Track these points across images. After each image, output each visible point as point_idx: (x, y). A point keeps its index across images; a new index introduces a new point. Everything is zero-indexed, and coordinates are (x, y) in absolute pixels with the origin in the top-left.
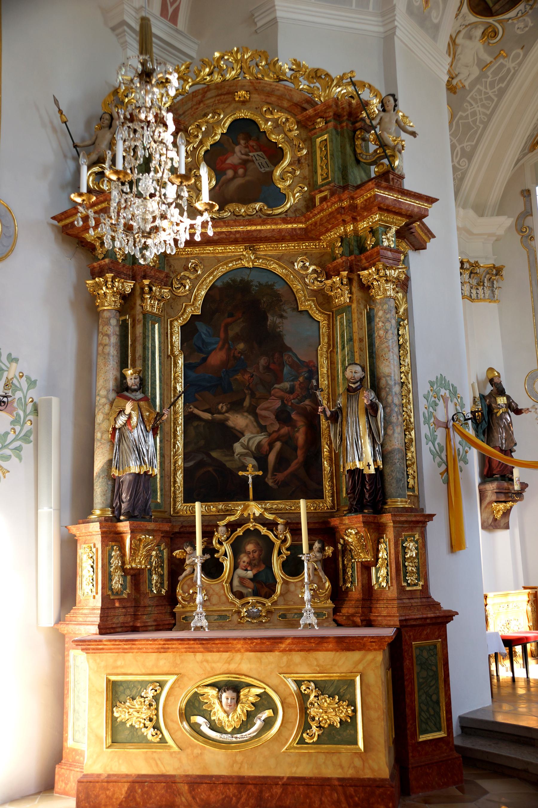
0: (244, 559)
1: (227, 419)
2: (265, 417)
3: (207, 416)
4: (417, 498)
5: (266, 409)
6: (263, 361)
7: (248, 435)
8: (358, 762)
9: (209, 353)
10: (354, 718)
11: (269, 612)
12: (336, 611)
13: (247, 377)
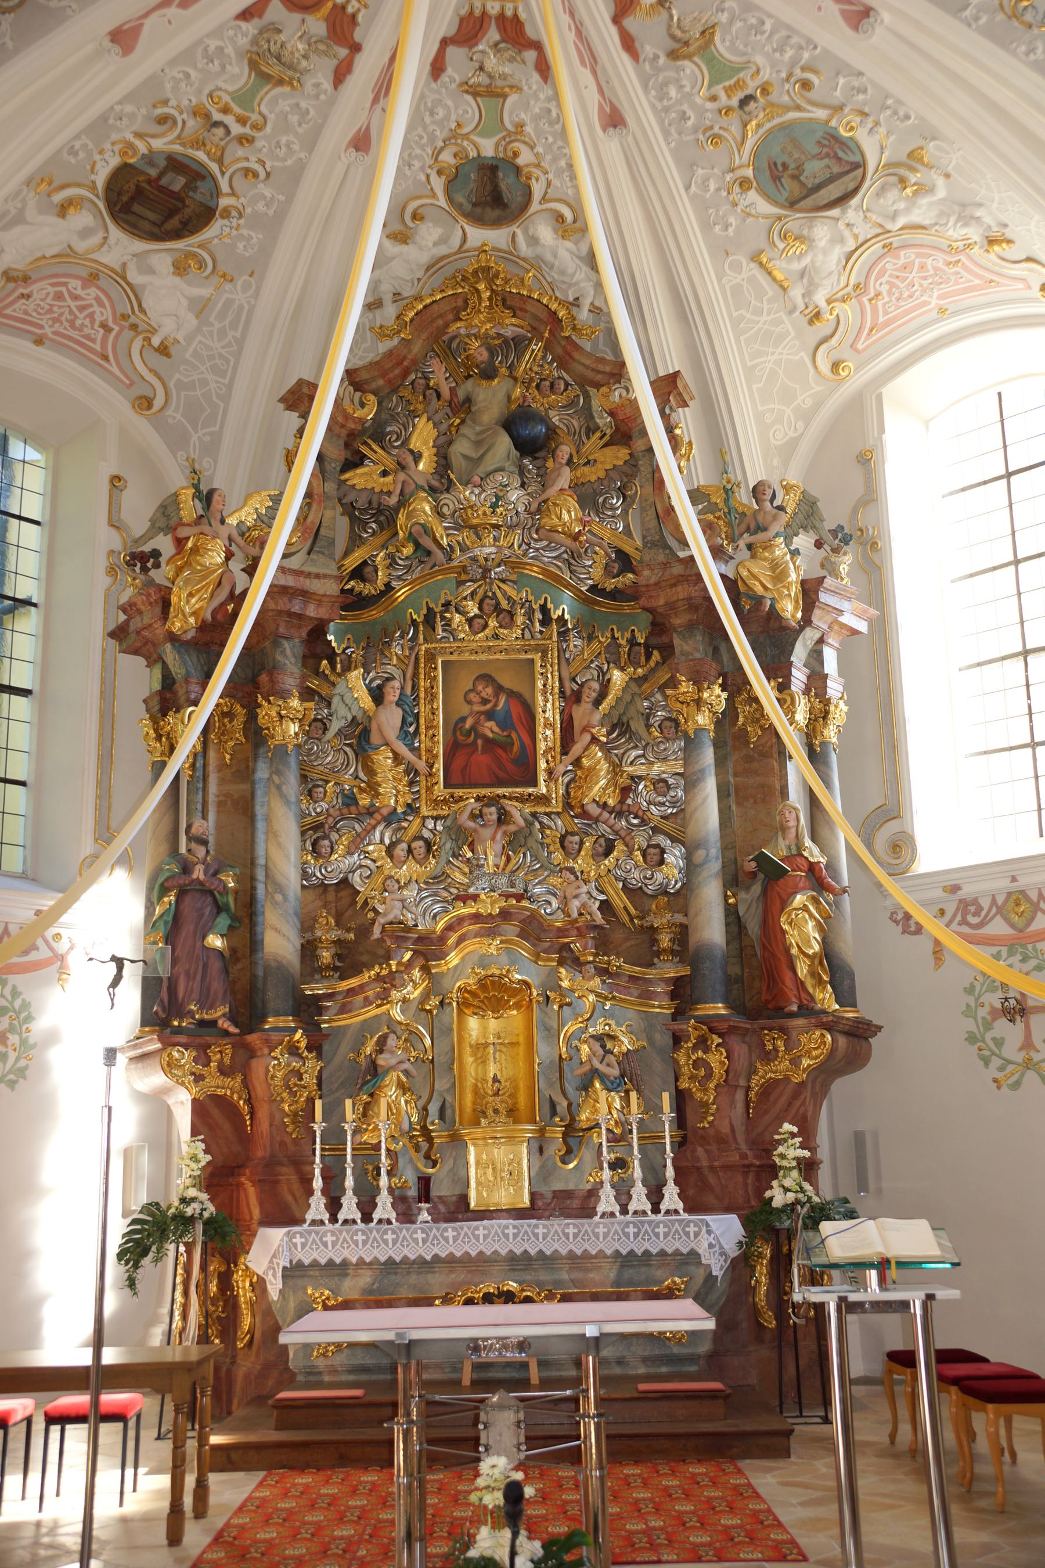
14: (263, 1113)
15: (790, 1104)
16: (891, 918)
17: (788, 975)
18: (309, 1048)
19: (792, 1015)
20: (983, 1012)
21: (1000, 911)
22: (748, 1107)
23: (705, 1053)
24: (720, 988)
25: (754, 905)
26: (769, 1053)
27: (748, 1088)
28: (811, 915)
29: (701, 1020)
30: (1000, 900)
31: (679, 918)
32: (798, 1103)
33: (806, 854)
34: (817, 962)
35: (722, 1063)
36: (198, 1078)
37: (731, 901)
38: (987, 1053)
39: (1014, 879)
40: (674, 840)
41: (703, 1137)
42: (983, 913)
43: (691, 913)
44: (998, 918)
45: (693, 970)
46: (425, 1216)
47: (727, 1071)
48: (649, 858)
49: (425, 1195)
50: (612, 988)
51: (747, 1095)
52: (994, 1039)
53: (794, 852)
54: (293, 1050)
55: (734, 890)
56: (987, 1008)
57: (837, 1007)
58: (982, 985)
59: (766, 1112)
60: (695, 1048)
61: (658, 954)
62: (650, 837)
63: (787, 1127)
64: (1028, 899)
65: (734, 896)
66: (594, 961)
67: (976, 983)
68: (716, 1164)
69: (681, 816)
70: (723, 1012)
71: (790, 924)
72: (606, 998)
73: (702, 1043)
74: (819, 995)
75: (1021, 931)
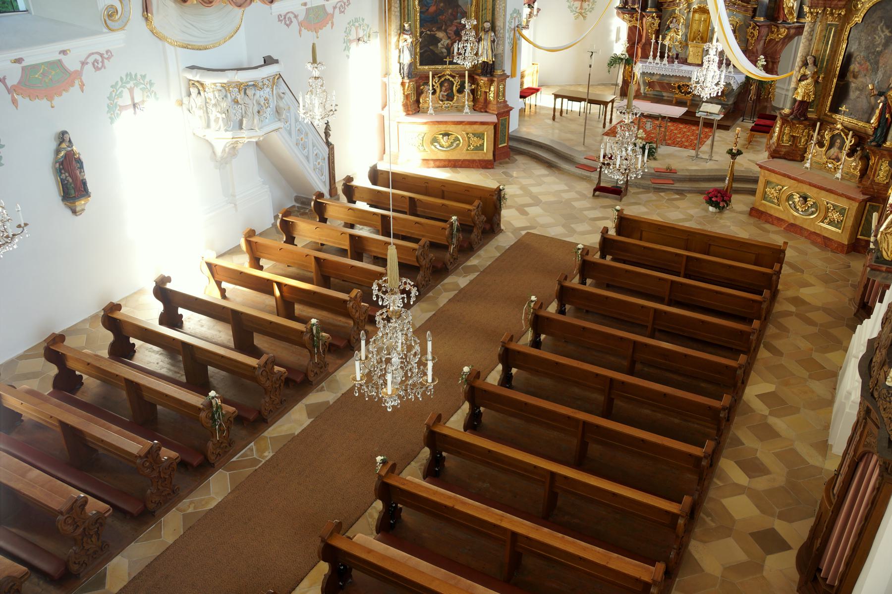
0: (444, 88)
1: (436, 34)
2: (449, 33)
3: (428, 32)
4: (504, 71)
5: (451, 30)
6: (450, 11)
7: (443, 40)
8: (484, 155)
9: (429, 7)
10: (483, 144)
11: (452, 106)
12: (473, 106)
13: (444, 17)
14: (645, 31)
17: (782, 12)
18: (657, 17)
24: (763, 13)
36: (630, 21)
46: (676, 62)
49: (677, 58)
54: (653, 17)
63: (762, 57)
73: (754, 28)
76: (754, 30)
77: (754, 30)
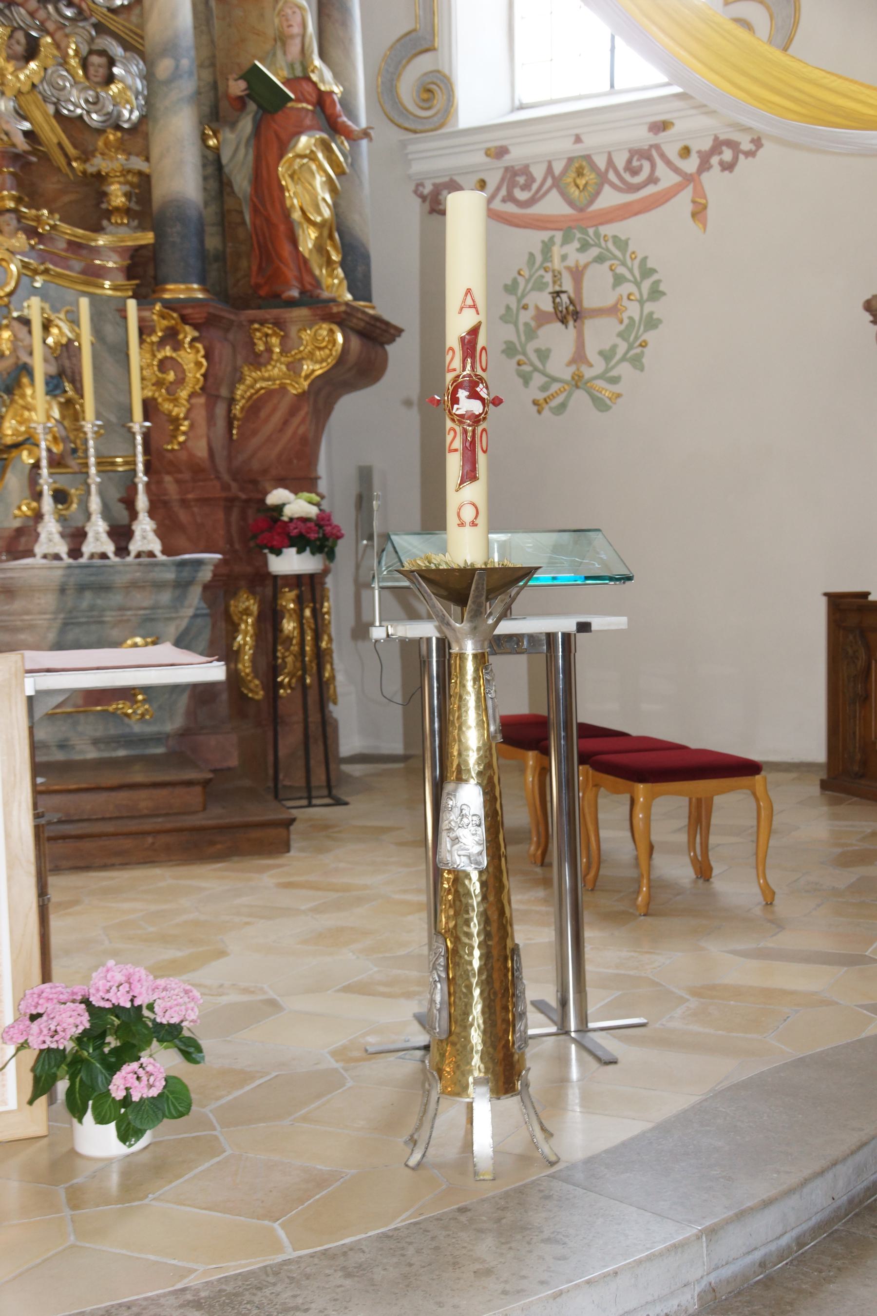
15: (286, 423)
16: (415, 192)
19: (292, 303)
20: (525, 317)
21: (557, 183)
22: (230, 427)
23: (175, 349)
25: (242, 151)
26: (258, 355)
27: (232, 401)
28: (321, 167)
29: (169, 305)
30: (558, 168)
31: (137, 163)
32: (296, 421)
33: (314, 77)
34: (326, 233)
35: (198, 364)
37: (212, 142)
38: (527, 368)
39: (578, 139)
40: (127, 46)
41: (171, 463)
42: (535, 187)
43: (155, 152)
44: (554, 193)
45: (157, 237)
47: (205, 376)
48: (92, 70)
50: (44, 256)
51: (229, 411)
52: (538, 351)
53: (299, 73)
55: (214, 125)
56: (531, 312)
57: (349, 297)
58: (527, 281)
59: (254, 433)
60: (162, 343)
61: (108, 214)
62: (92, 39)
64: (593, 167)
65: (215, 135)
66: (15, 211)
67: (520, 279)
68: (190, 496)
69: (136, 11)
70: (200, 296)
71: (292, 176)
72: (36, 272)
73: (171, 337)
74: (326, 281)
75: (581, 210)
76: (177, 346)
77: (177, 346)
